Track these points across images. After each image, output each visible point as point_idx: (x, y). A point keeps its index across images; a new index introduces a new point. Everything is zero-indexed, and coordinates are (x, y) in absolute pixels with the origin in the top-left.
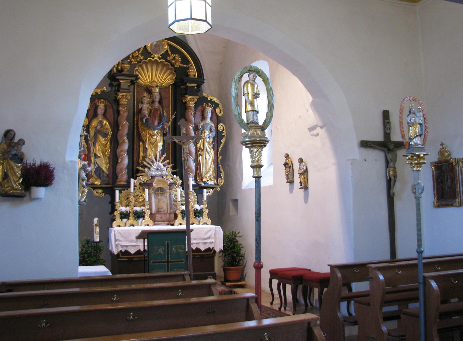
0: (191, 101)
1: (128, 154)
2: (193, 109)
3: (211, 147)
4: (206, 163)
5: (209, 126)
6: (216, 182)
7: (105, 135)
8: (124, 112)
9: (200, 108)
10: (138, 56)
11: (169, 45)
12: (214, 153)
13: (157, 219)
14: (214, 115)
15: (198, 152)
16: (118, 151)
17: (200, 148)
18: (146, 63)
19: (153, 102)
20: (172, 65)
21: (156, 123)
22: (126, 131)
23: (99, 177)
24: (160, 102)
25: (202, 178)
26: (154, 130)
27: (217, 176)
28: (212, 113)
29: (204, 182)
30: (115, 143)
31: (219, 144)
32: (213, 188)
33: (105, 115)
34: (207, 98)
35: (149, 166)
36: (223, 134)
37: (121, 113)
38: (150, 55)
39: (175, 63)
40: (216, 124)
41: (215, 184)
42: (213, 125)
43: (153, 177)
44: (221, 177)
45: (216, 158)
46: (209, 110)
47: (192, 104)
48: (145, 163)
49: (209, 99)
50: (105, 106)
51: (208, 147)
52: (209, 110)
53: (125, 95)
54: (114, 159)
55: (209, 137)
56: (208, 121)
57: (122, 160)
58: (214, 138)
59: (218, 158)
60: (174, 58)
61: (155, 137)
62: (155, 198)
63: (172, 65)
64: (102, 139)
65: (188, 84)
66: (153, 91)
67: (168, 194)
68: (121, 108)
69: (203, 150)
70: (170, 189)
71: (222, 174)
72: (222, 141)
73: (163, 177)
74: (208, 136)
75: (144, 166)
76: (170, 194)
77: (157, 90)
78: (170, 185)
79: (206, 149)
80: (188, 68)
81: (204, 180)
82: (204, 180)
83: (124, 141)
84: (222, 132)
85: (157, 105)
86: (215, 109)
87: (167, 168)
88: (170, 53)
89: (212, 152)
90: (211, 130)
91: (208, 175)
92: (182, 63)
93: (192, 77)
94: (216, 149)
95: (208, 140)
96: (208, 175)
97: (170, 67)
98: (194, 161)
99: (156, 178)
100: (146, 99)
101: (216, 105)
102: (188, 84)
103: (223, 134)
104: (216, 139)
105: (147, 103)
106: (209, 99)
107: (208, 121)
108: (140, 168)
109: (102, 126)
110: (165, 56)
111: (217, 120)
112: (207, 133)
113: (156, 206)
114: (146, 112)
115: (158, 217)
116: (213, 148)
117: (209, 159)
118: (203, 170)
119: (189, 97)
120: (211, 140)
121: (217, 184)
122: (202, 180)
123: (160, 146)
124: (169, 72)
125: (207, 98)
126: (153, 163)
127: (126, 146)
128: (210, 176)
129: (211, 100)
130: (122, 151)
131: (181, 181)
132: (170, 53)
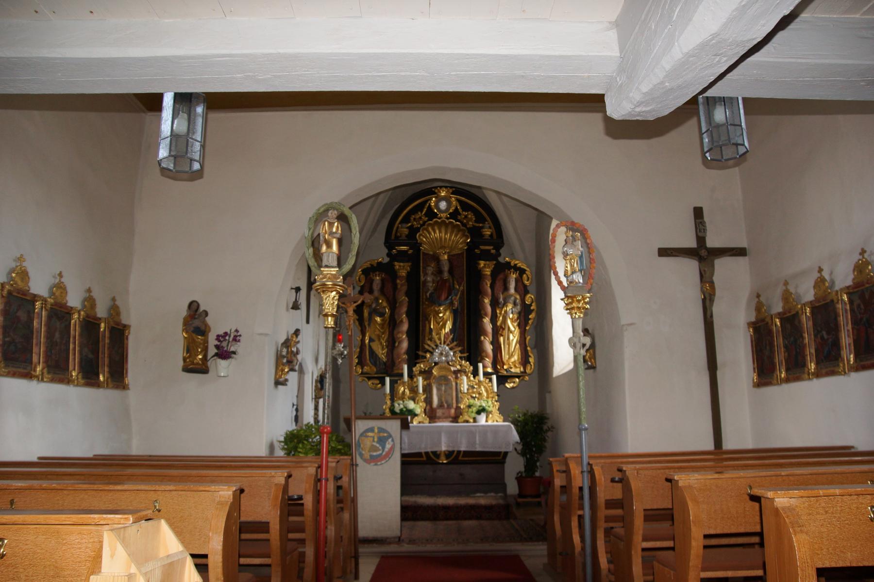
0: (486, 268)
1: (408, 336)
2: (490, 278)
3: (515, 324)
4: (509, 345)
5: (513, 298)
6: (522, 369)
7: (381, 315)
8: (402, 285)
9: (501, 276)
10: (420, 218)
11: (458, 200)
13: (438, 415)
14: (520, 284)
15: (498, 331)
16: (395, 332)
17: (501, 327)
18: (433, 226)
19: (440, 272)
20: (464, 225)
21: (443, 297)
22: (405, 309)
23: (375, 364)
24: (451, 271)
25: (504, 364)
26: (440, 305)
27: (525, 361)
28: (517, 281)
30: (393, 324)
31: (527, 320)
32: (518, 377)
33: (382, 291)
34: (509, 263)
35: (430, 349)
37: (399, 287)
38: (435, 215)
39: (468, 222)
42: (518, 297)
43: (436, 364)
46: (513, 276)
47: (488, 272)
48: (427, 347)
49: (512, 264)
50: (383, 280)
51: (512, 326)
52: (513, 276)
53: (402, 264)
54: (392, 344)
56: (512, 291)
57: (399, 343)
58: (519, 313)
59: (525, 339)
60: (466, 217)
61: (441, 315)
62: (438, 389)
63: (464, 225)
64: (378, 319)
65: (482, 247)
66: (441, 258)
67: (454, 384)
68: (398, 281)
69: (504, 329)
70: (457, 378)
71: (531, 360)
73: (448, 363)
75: (428, 351)
76: (456, 384)
77: (446, 257)
78: (456, 373)
79: (509, 328)
80: (482, 228)
82: (505, 367)
83: (402, 321)
84: (531, 305)
85: (446, 275)
86: (521, 275)
87: (454, 353)
88: (460, 210)
89: (517, 332)
90: (515, 304)
91: (513, 360)
92: (476, 221)
93: (487, 237)
95: (511, 316)
96: (513, 360)
97: (462, 228)
98: (492, 343)
99: (440, 364)
100: (430, 270)
101: (522, 271)
102: (482, 247)
105: (432, 274)
106: (512, 264)
107: (512, 291)
108: (420, 353)
109: (378, 304)
110: (454, 215)
111: (523, 290)
112: (510, 307)
113: (440, 400)
114: (431, 286)
115: (439, 413)
116: (519, 325)
118: (505, 357)
119: (482, 263)
120: (516, 316)
121: (525, 372)
123: (449, 326)
124: (460, 233)
125: (509, 263)
126: (437, 346)
127: (405, 327)
129: (515, 265)
130: (399, 332)
131: (472, 368)
132: (460, 210)
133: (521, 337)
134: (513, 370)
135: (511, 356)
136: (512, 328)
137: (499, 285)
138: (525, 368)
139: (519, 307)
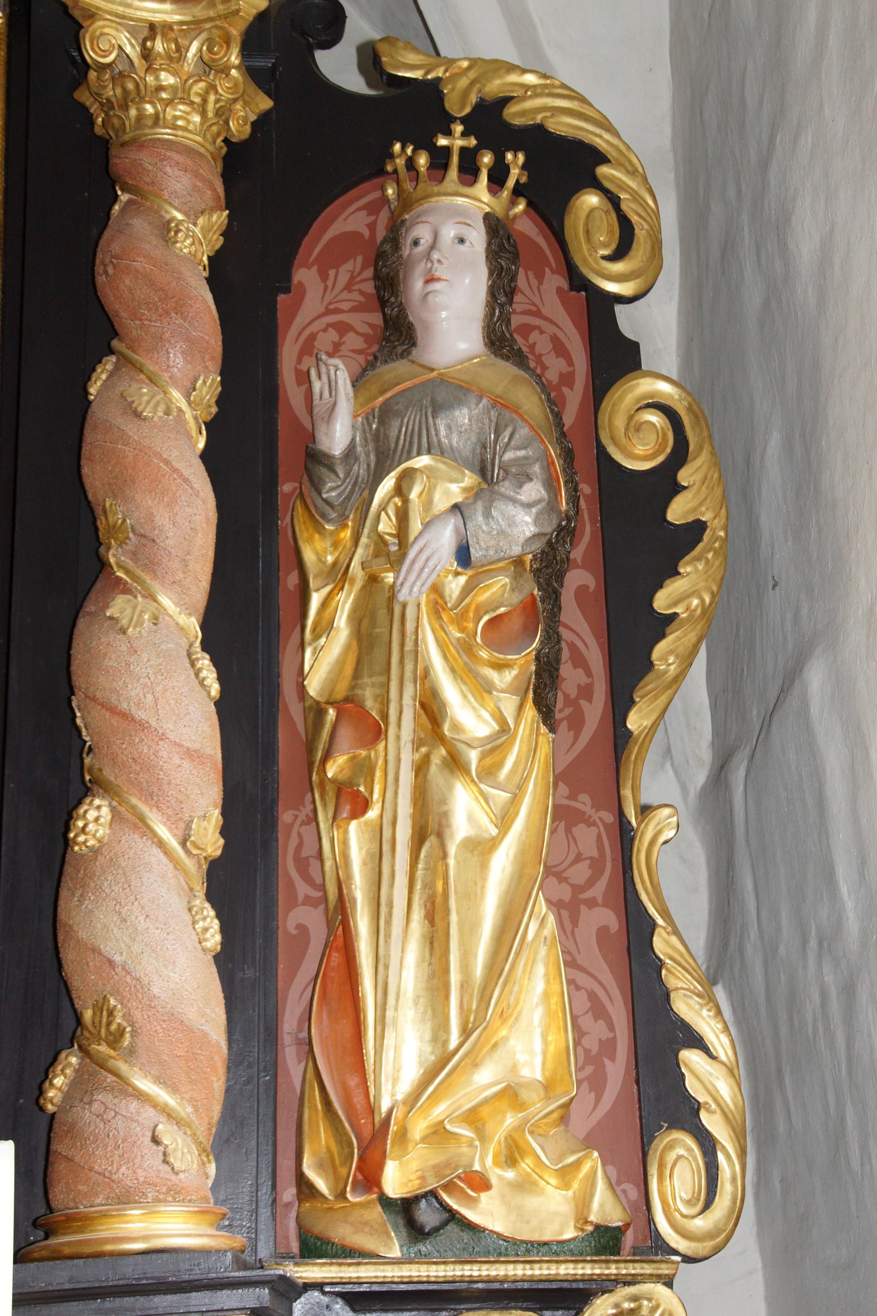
9: (350, 218)
12: (566, 777)
14: (544, 294)
29: (404, 1210)
36: (678, 511)
40: (574, 399)
41: (605, 1241)
44: (685, 1113)
45: (590, 839)
55: (463, 555)
58: (547, 565)
69: (375, 732)
71: (710, 1077)
72: (662, 601)
74: (445, 538)
79: (431, 710)
81: (396, 1180)
82: (396, 1180)
84: (665, 481)
89: (531, 752)
94: (595, 710)
103: (678, 511)
104: (580, 579)
116: (544, 689)
117: (481, 848)
120: (499, 590)
122: (370, 1179)
128: (510, 1095)
133: (564, 816)
134: (488, 1212)
135: (468, 1024)
136: (470, 718)
137: (320, 296)
138: (635, 1173)
139: (533, 490)
